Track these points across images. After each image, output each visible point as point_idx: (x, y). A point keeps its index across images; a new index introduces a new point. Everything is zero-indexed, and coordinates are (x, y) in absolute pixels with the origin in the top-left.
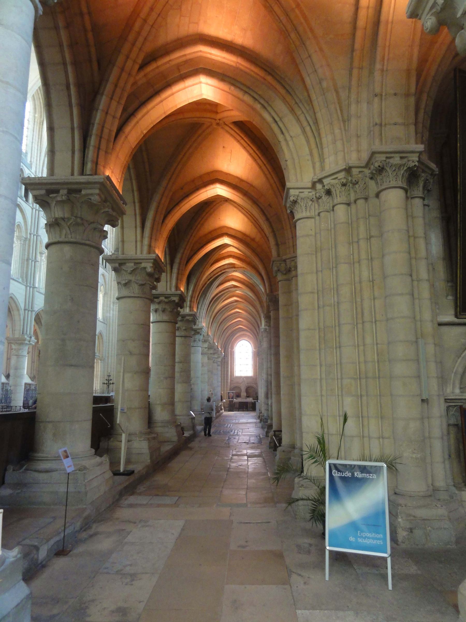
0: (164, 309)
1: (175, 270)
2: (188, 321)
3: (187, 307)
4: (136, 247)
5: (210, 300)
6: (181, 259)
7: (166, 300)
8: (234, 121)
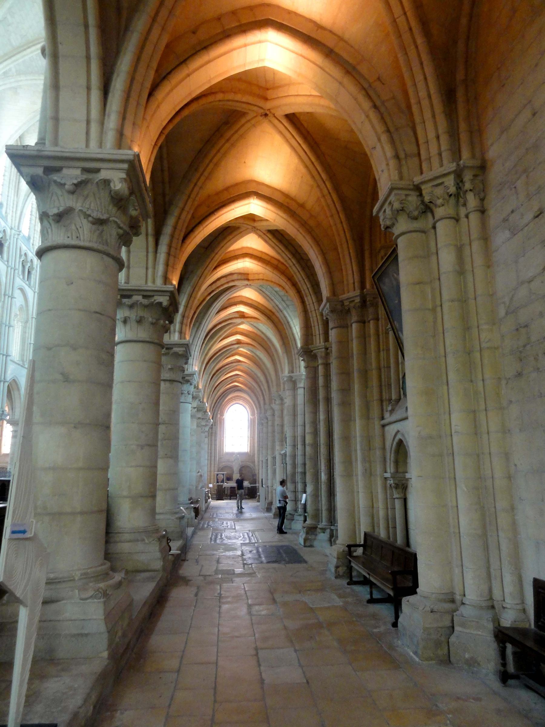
0: (141, 317)
1: (163, 248)
2: (177, 355)
3: (175, 332)
4: (88, 133)
6: (175, 228)
7: (145, 302)
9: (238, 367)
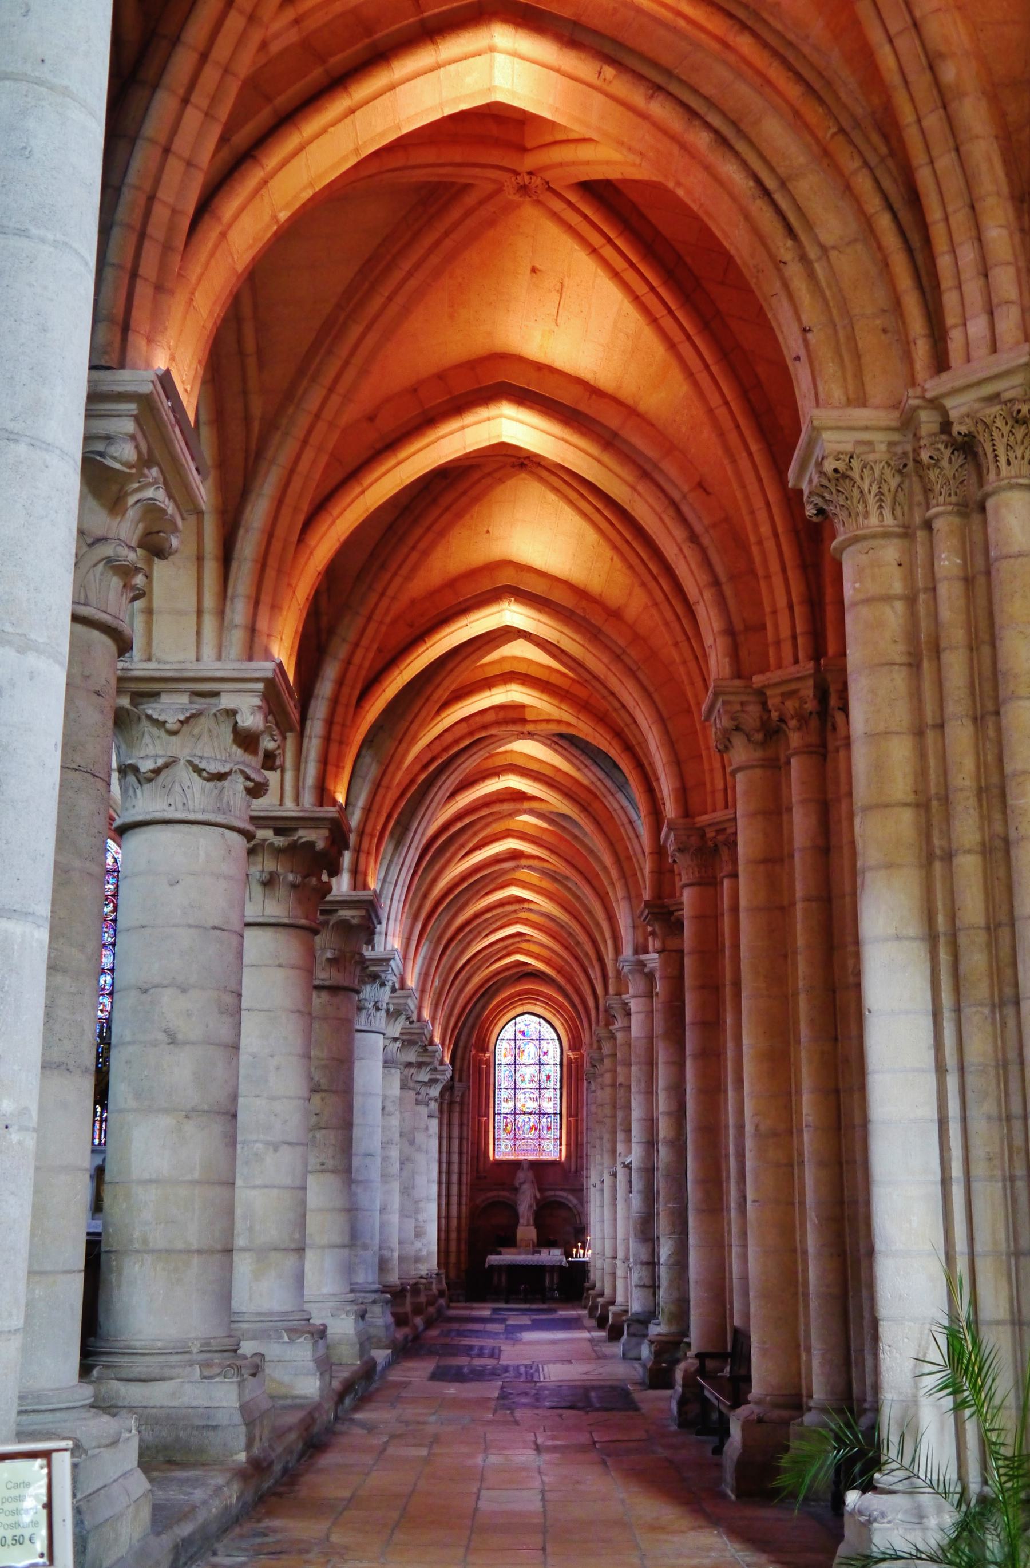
0: (271, 874)
2: (344, 926)
4: (199, 633)
6: (340, 683)
7: (280, 841)
8: (584, 178)
9: (523, 915)
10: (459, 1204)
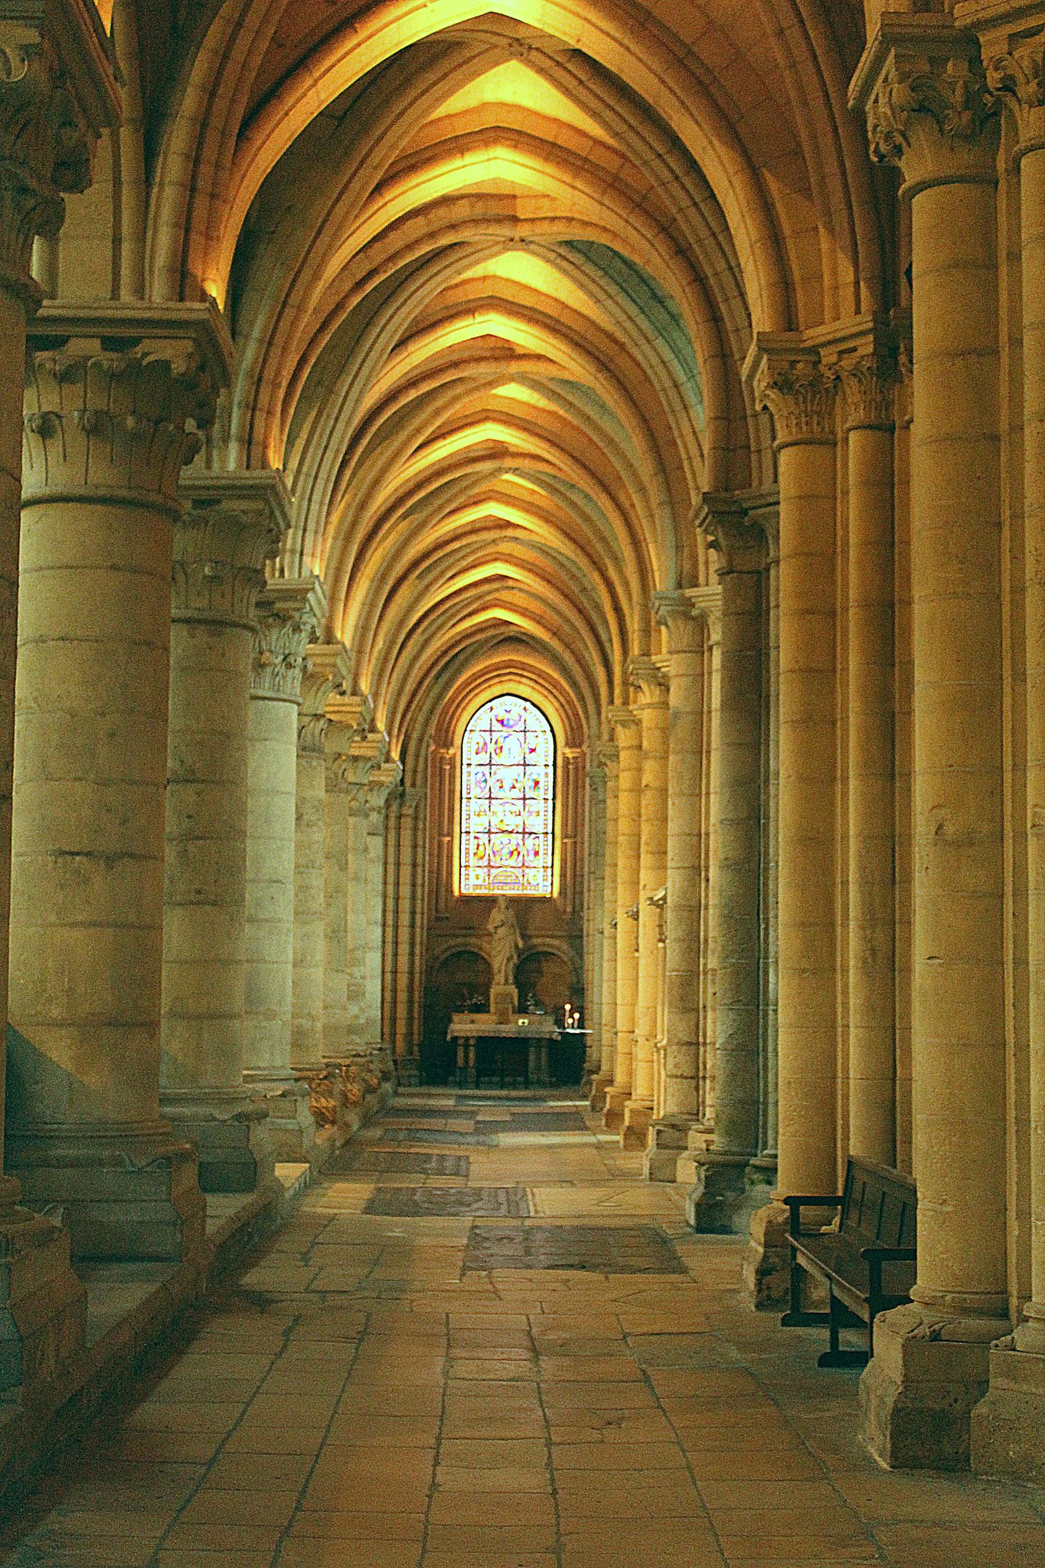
3: (226, 440)
5: (356, 421)
6: (211, 92)
7: (111, 360)
9: (505, 547)
10: (412, 954)
